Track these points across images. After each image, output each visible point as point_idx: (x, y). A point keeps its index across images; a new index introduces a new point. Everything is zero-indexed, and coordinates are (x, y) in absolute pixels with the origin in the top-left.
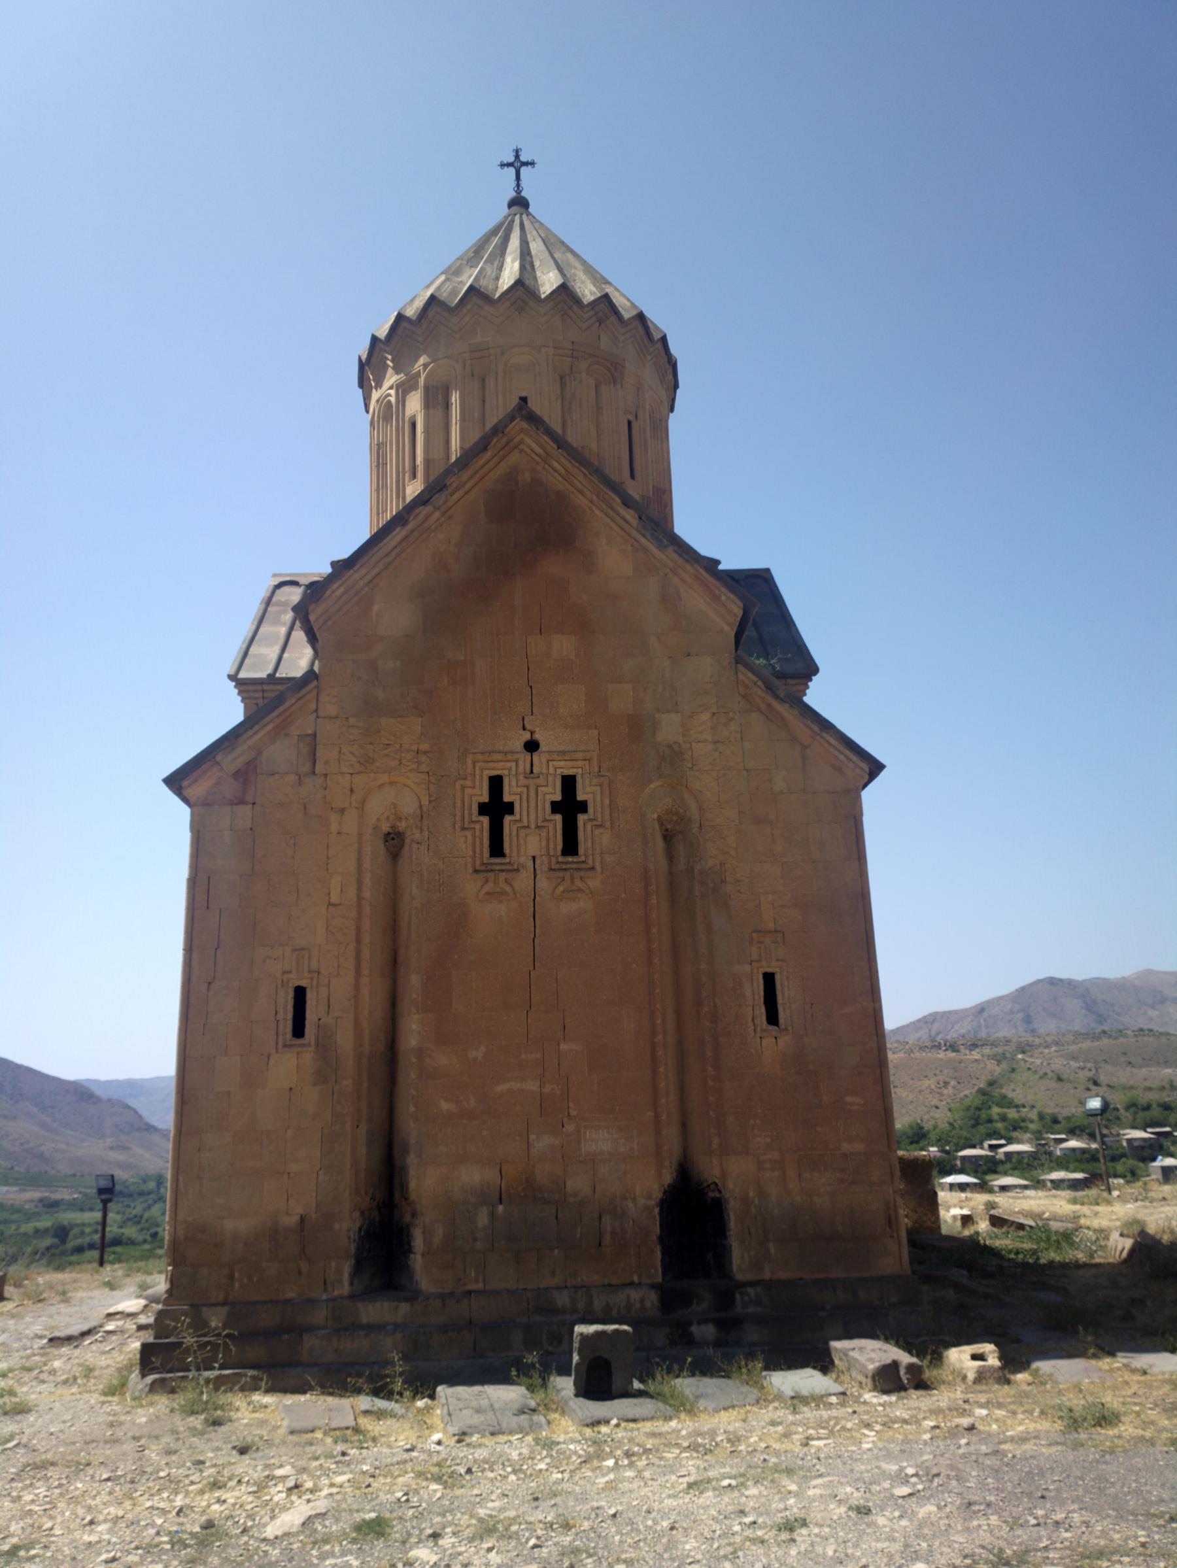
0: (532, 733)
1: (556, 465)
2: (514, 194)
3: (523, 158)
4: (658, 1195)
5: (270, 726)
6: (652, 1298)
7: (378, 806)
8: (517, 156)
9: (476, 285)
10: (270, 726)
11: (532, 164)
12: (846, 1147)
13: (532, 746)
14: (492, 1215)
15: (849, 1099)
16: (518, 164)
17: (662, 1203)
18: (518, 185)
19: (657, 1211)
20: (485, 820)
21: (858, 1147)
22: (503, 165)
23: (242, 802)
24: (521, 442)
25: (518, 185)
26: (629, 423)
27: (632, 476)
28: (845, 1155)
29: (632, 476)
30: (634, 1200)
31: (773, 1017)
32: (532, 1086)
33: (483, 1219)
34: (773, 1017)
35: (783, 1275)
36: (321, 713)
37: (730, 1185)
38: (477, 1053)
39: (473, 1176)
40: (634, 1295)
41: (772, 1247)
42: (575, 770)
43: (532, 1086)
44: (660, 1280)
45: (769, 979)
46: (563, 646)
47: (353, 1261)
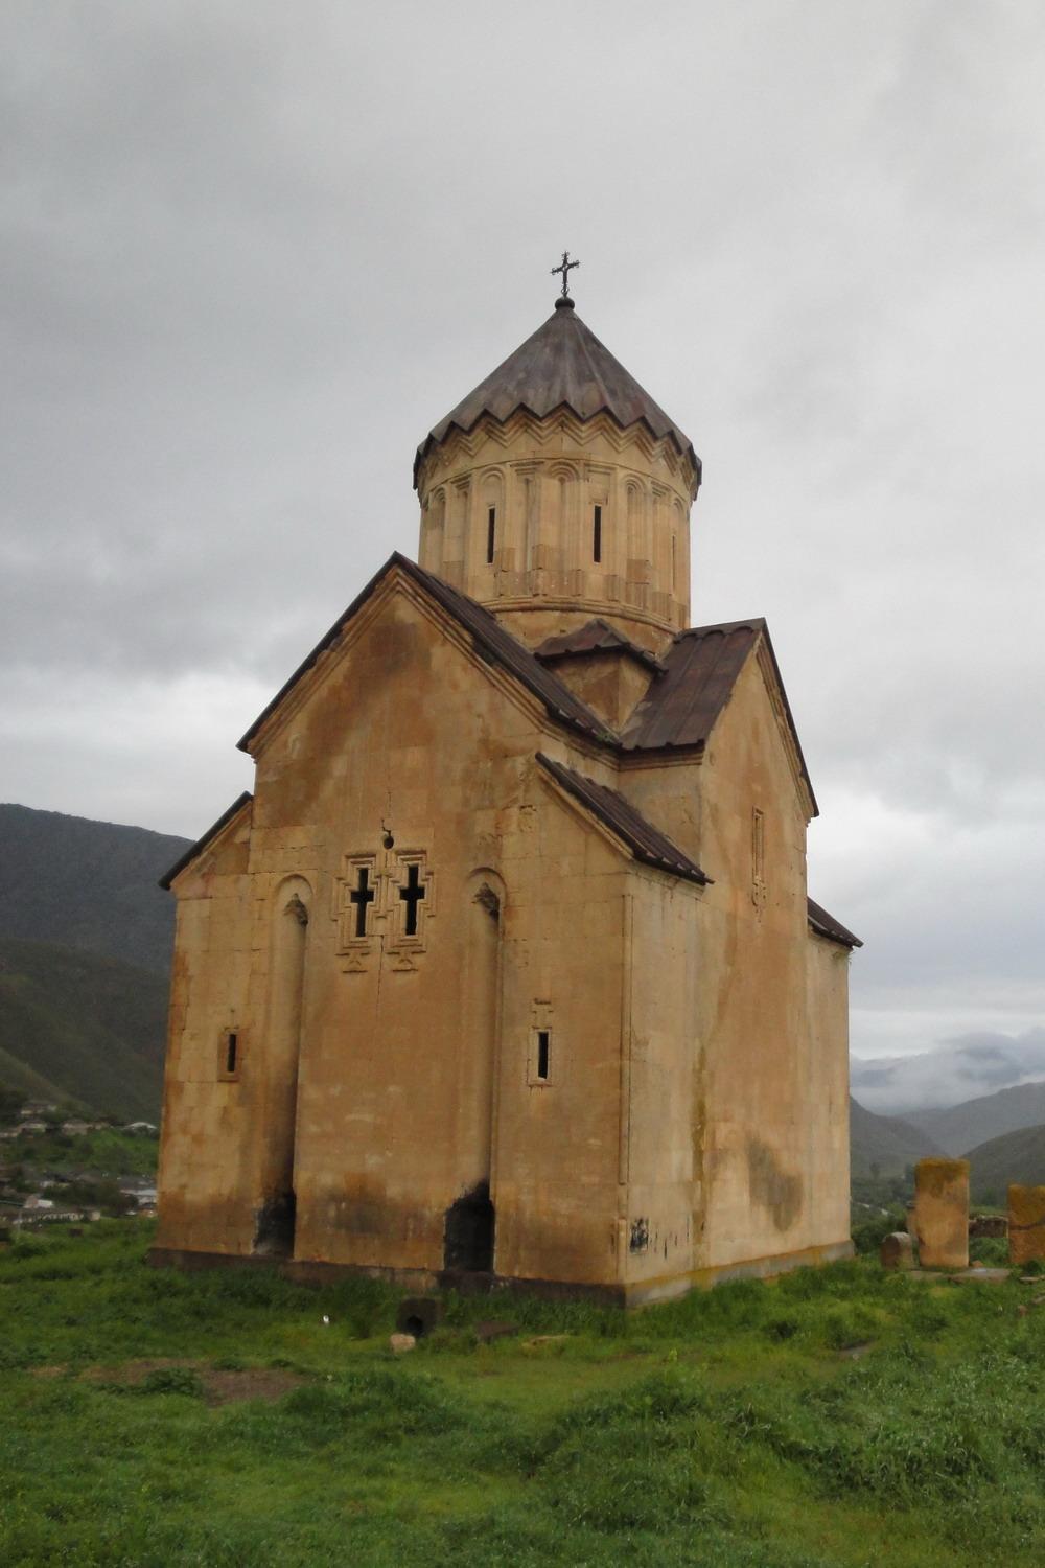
0: (389, 832)
1: (420, 600)
2: (561, 296)
3: (570, 262)
4: (448, 1204)
5: (221, 837)
6: (433, 1282)
7: (286, 896)
8: (565, 262)
9: (456, 421)
10: (221, 837)
11: (576, 264)
12: (585, 1179)
13: (389, 843)
14: (338, 1210)
15: (592, 1141)
16: (566, 266)
17: (450, 1213)
18: (565, 287)
19: (444, 1218)
20: (355, 906)
21: (595, 1179)
22: (554, 271)
23: (205, 897)
24: (398, 583)
25: (565, 287)
26: (598, 511)
27: (597, 558)
28: (583, 1186)
29: (597, 558)
30: (430, 1208)
31: (543, 1072)
32: (368, 1118)
33: (332, 1212)
34: (543, 1072)
35: (528, 1276)
36: (254, 825)
37: (497, 1203)
38: (336, 1091)
39: (327, 1180)
40: (423, 1279)
41: (522, 1253)
42: (416, 862)
43: (368, 1118)
44: (442, 1268)
45: (544, 1038)
46: (414, 757)
47: (257, 1232)
